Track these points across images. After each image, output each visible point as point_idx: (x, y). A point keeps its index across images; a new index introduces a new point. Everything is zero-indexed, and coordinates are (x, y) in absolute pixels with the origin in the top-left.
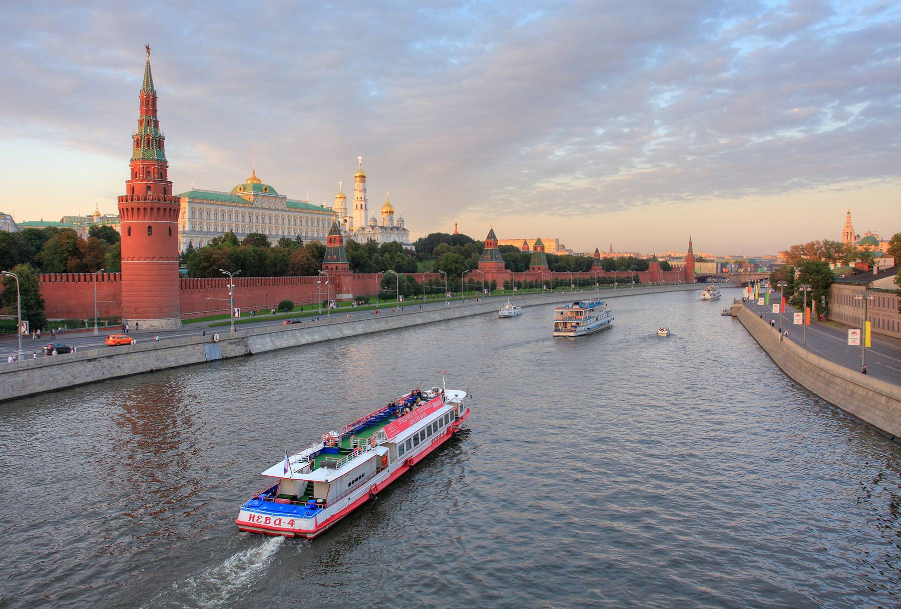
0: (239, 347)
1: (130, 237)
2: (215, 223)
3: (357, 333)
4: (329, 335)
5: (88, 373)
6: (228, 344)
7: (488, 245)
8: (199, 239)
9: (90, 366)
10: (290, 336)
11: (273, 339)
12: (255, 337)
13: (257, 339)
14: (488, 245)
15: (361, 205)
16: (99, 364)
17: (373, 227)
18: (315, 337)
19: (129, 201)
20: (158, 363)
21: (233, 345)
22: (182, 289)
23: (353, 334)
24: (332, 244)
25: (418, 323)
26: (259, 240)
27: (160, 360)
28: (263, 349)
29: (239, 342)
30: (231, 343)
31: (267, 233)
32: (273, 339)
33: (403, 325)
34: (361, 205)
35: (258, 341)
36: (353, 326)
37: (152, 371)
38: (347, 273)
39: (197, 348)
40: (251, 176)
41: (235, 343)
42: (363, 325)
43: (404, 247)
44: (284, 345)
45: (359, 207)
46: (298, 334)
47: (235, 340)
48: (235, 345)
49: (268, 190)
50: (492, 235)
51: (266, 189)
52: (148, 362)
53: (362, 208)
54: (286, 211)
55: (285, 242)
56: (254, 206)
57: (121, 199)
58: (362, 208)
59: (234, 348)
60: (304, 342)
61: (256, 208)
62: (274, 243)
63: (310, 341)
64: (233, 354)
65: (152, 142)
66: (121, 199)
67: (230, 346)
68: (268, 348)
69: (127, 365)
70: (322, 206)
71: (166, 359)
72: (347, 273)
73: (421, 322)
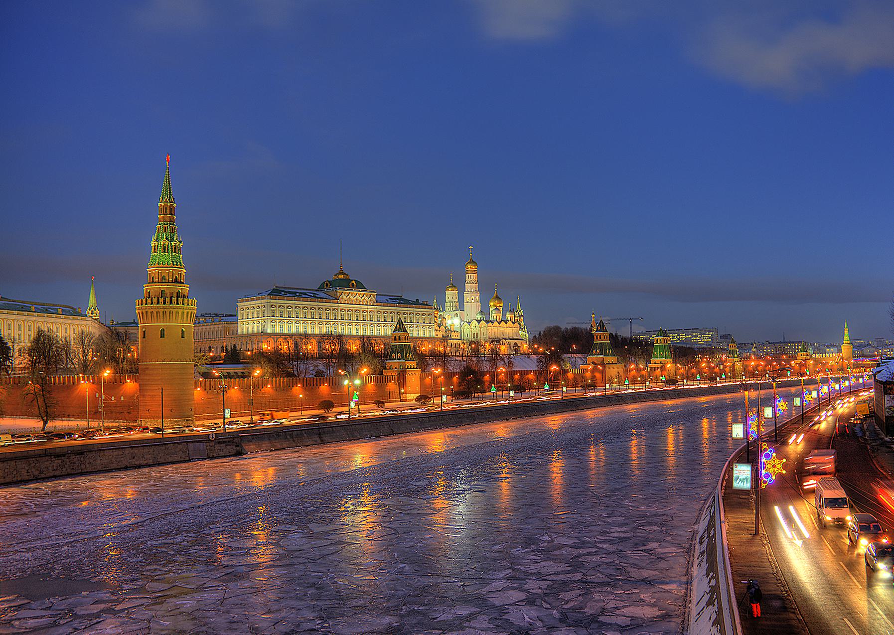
0: (229, 447)
1: (144, 339)
5: (55, 468)
7: (597, 339)
9: (58, 462)
14: (597, 339)
16: (68, 460)
17: (479, 321)
20: (134, 460)
24: (397, 341)
27: (136, 458)
29: (229, 442)
39: (180, 446)
41: (224, 442)
48: (224, 445)
52: (122, 459)
65: (168, 247)
69: (99, 462)
70: (417, 300)
71: (143, 457)
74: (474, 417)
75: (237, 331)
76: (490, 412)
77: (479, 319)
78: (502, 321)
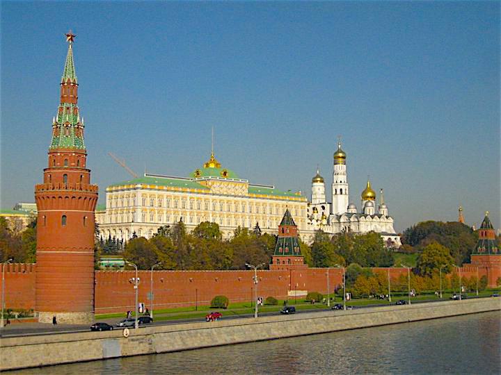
2: (191, 213)
3: (288, 334)
4: (253, 335)
6: (129, 340)
8: (149, 228)
11: (184, 337)
12: (162, 335)
13: (165, 336)
15: (341, 190)
18: (235, 337)
19: (45, 190)
20: (49, 357)
21: (135, 342)
23: (283, 335)
26: (208, 231)
27: (51, 354)
30: (133, 340)
31: (218, 222)
34: (341, 190)
35: (165, 339)
37: (40, 367)
39: (94, 343)
41: (137, 340)
42: (297, 325)
43: (386, 238)
44: (196, 345)
45: (339, 192)
48: (138, 342)
50: (486, 225)
53: (341, 193)
54: (247, 197)
57: (38, 187)
58: (341, 193)
62: (228, 235)
64: (135, 352)
66: (38, 187)
67: (131, 342)
76: (392, 312)
77: (350, 212)
78: (375, 215)
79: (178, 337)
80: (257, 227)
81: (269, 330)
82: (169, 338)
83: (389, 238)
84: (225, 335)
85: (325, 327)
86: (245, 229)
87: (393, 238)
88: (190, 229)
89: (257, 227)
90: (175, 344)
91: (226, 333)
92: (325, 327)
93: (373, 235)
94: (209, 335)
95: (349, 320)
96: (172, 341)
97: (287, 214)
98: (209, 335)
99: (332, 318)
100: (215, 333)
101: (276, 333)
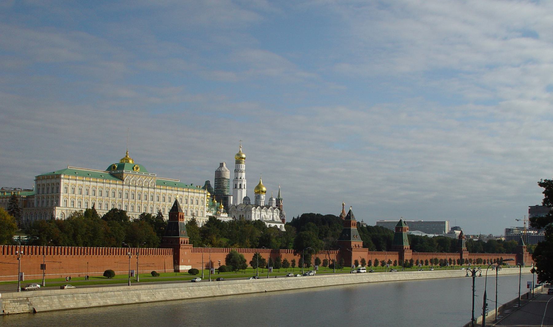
0: (23, 305)
3: (156, 300)
4: (124, 299)
10: (81, 298)
11: (61, 300)
13: (44, 299)
18: (108, 301)
21: (16, 304)
22: (4, 254)
23: (151, 300)
25: (229, 293)
28: (49, 309)
30: (14, 301)
32: (61, 300)
33: (211, 295)
34: (240, 185)
35: (45, 301)
36: (153, 293)
38: (187, 247)
40: (124, 156)
41: (17, 301)
43: (267, 224)
45: (239, 187)
46: (90, 297)
47: (18, 299)
48: (19, 303)
49: (139, 169)
51: (137, 168)
55: (145, 217)
56: (124, 183)
59: (17, 306)
60: (94, 304)
61: (126, 185)
63: (102, 304)
67: (13, 303)
68: (54, 308)
72: (187, 247)
73: (232, 293)
74: (238, 288)
75: (33, 204)
76: (251, 284)
79: (56, 300)
80: (160, 213)
81: (139, 296)
82: (48, 301)
83: (276, 225)
84: (99, 299)
85: (190, 294)
86: (149, 215)
87: (279, 226)
88: (101, 212)
89: (160, 213)
90: (53, 305)
91: (100, 297)
92: (190, 294)
93: (259, 224)
94: (86, 298)
95: (212, 289)
96: (51, 303)
97: (176, 202)
98: (86, 298)
99: (197, 288)
100: (90, 297)
101: (144, 298)
